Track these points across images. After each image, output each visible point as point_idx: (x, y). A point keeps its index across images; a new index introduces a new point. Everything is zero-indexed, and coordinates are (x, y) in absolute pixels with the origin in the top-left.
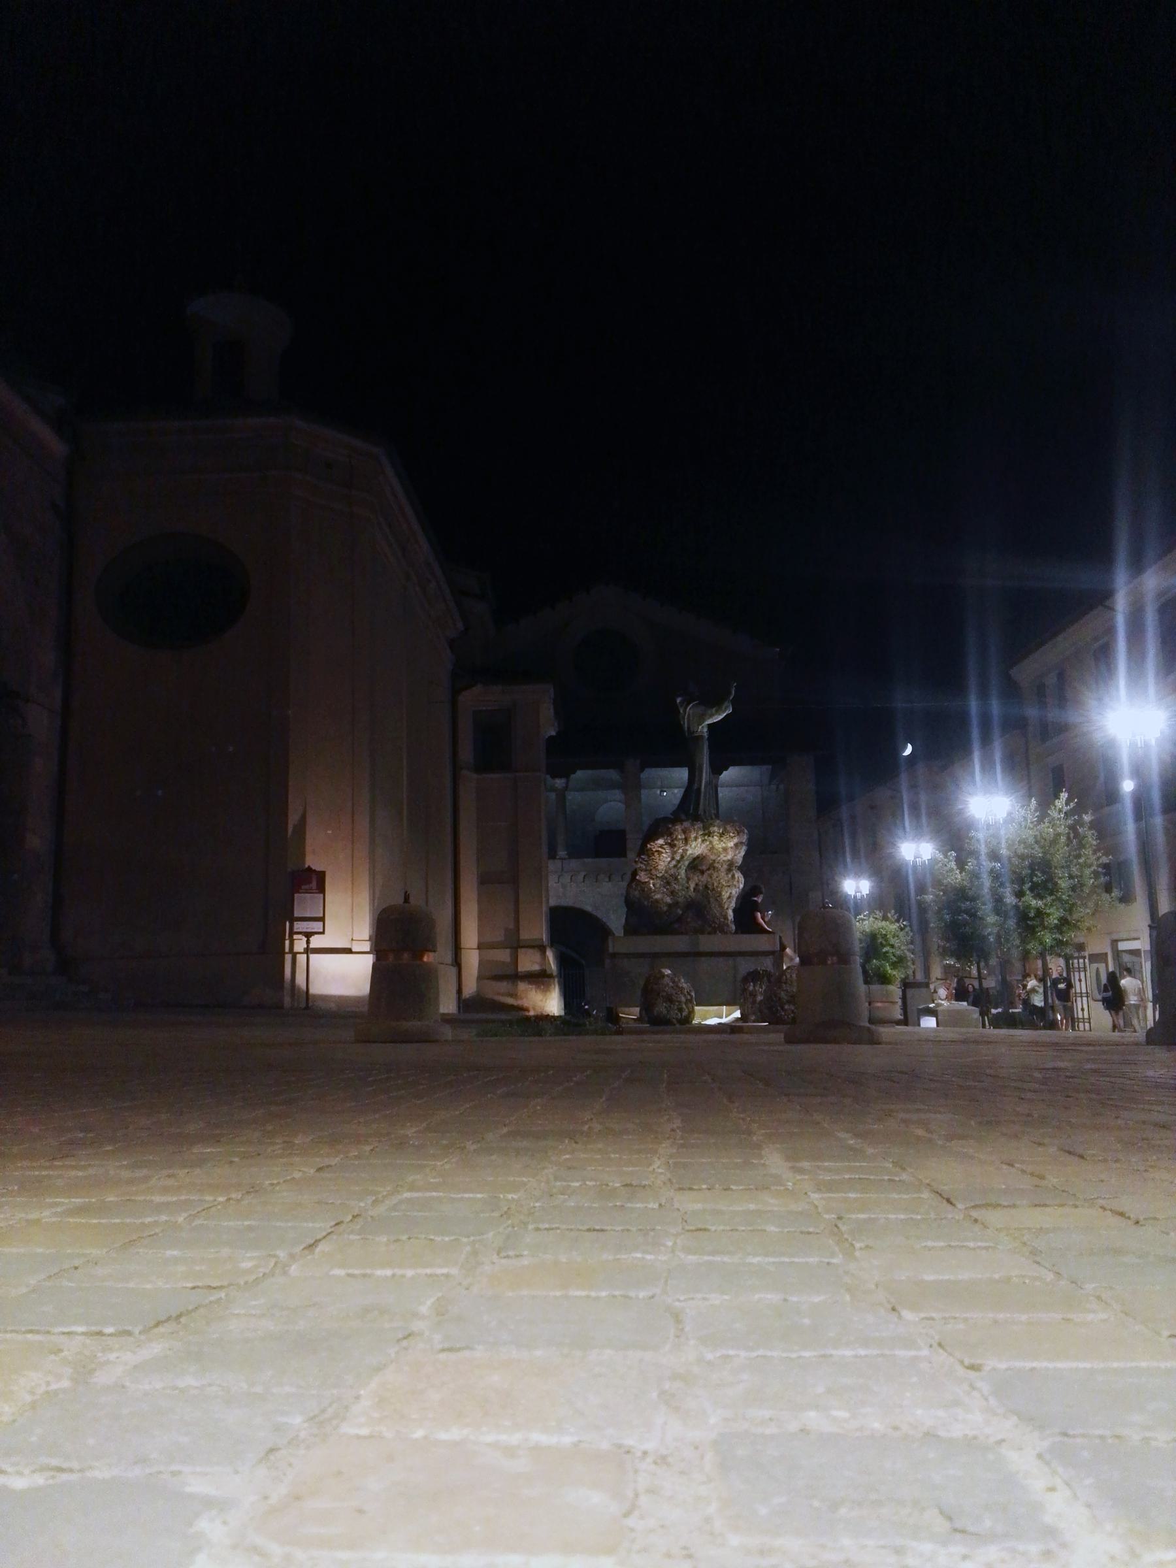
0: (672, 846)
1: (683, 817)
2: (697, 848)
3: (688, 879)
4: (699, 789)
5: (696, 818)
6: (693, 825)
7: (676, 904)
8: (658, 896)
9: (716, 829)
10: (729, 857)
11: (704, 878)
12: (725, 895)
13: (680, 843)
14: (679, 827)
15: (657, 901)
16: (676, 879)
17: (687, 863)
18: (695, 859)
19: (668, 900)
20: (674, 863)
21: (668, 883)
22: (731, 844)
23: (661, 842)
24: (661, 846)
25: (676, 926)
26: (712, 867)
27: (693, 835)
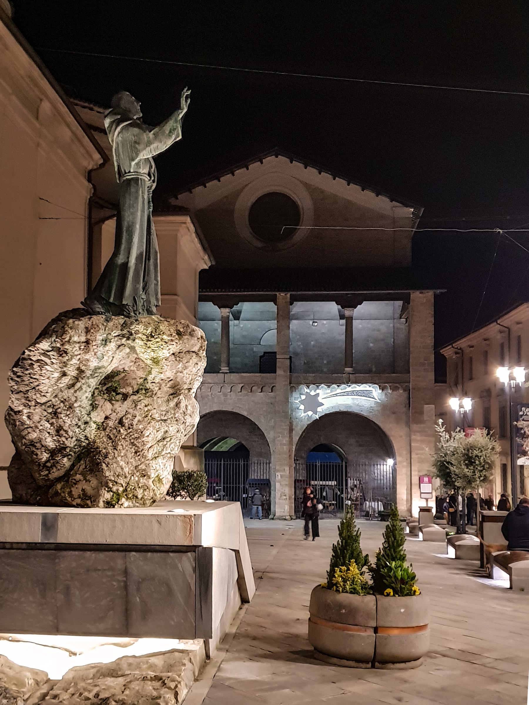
0: (62, 352)
1: (98, 307)
2: (108, 356)
3: (94, 407)
4: (125, 266)
5: (119, 310)
6: (107, 321)
7: (61, 450)
8: (34, 436)
9: (140, 328)
10: (169, 374)
11: (121, 408)
12: (151, 435)
13: (74, 349)
14: (82, 324)
15: (32, 443)
16: (71, 407)
17: (93, 382)
18: (110, 377)
19: (50, 442)
20: (66, 380)
21: (55, 414)
22: (164, 353)
23: (44, 345)
24: (45, 354)
25: (59, 486)
26: (143, 390)
27: (100, 337)
